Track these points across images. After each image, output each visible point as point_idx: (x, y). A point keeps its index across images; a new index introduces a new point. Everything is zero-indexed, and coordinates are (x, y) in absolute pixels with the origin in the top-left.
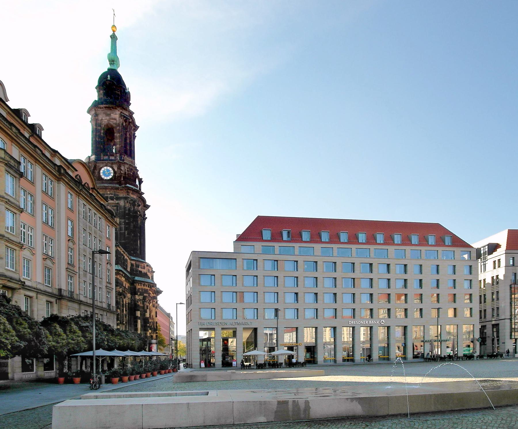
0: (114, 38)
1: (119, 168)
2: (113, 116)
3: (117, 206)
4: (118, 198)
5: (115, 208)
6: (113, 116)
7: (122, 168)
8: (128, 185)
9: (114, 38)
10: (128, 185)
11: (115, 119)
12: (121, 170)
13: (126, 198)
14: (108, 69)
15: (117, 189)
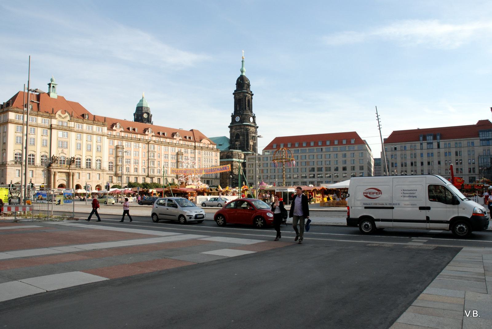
0: (243, 61)
1: (242, 116)
2: (240, 95)
3: (241, 131)
4: (241, 129)
5: (240, 132)
6: (240, 95)
7: (243, 116)
8: (244, 123)
9: (243, 61)
10: (244, 123)
11: (241, 96)
12: (242, 117)
13: (244, 128)
14: (241, 75)
15: (240, 125)
